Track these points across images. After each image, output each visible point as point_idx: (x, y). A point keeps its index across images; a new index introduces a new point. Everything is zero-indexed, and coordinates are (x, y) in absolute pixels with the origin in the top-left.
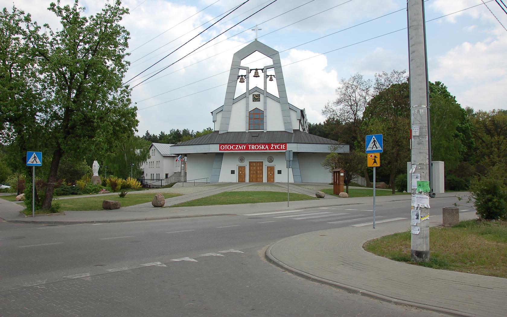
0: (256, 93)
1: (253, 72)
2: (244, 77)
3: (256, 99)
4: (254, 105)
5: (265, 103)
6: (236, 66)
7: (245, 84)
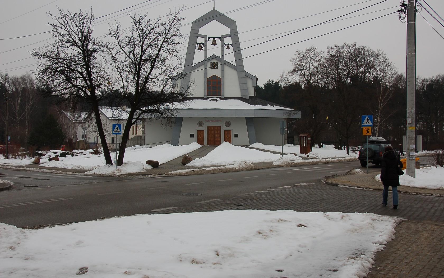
0: (214, 61)
1: (211, 41)
2: (202, 45)
3: (214, 66)
4: (212, 73)
5: (223, 71)
6: (194, 34)
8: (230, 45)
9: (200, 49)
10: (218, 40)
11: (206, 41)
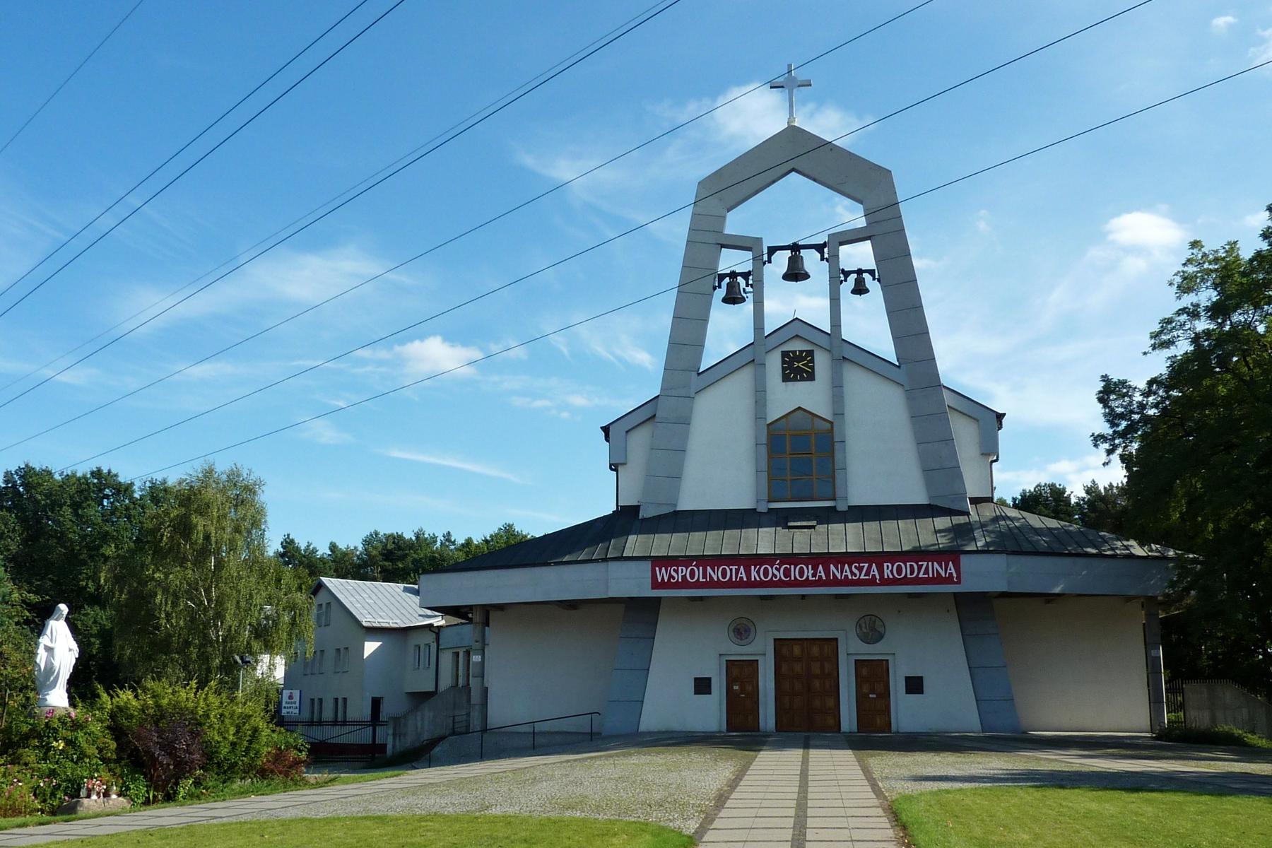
0: (797, 346)
1: (782, 259)
3: (797, 367)
4: (787, 398)
5: (837, 387)
6: (707, 237)
7: (748, 307)
8: (865, 275)
9: (733, 298)
10: (810, 260)
11: (759, 262)
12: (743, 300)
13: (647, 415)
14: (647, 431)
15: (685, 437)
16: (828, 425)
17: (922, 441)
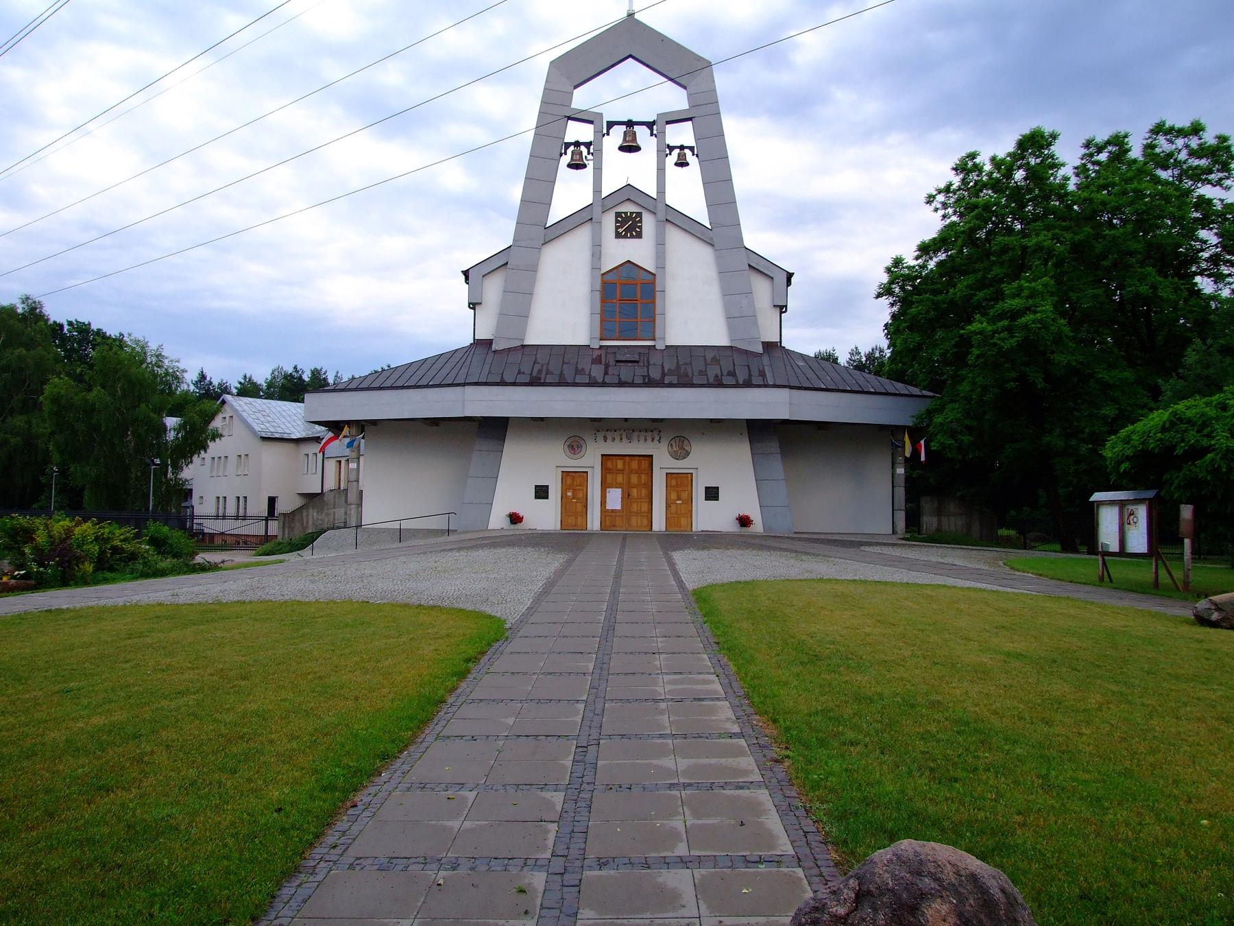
0: (629, 208)
1: (618, 134)
2: (583, 149)
3: (629, 227)
4: (619, 251)
5: (660, 244)
6: (556, 112)
7: (589, 171)
8: (687, 151)
9: (577, 165)
10: (642, 133)
11: (600, 135)
12: (584, 166)
13: (500, 263)
14: (504, 274)
15: (533, 283)
16: (651, 277)
17: (664, 253)
